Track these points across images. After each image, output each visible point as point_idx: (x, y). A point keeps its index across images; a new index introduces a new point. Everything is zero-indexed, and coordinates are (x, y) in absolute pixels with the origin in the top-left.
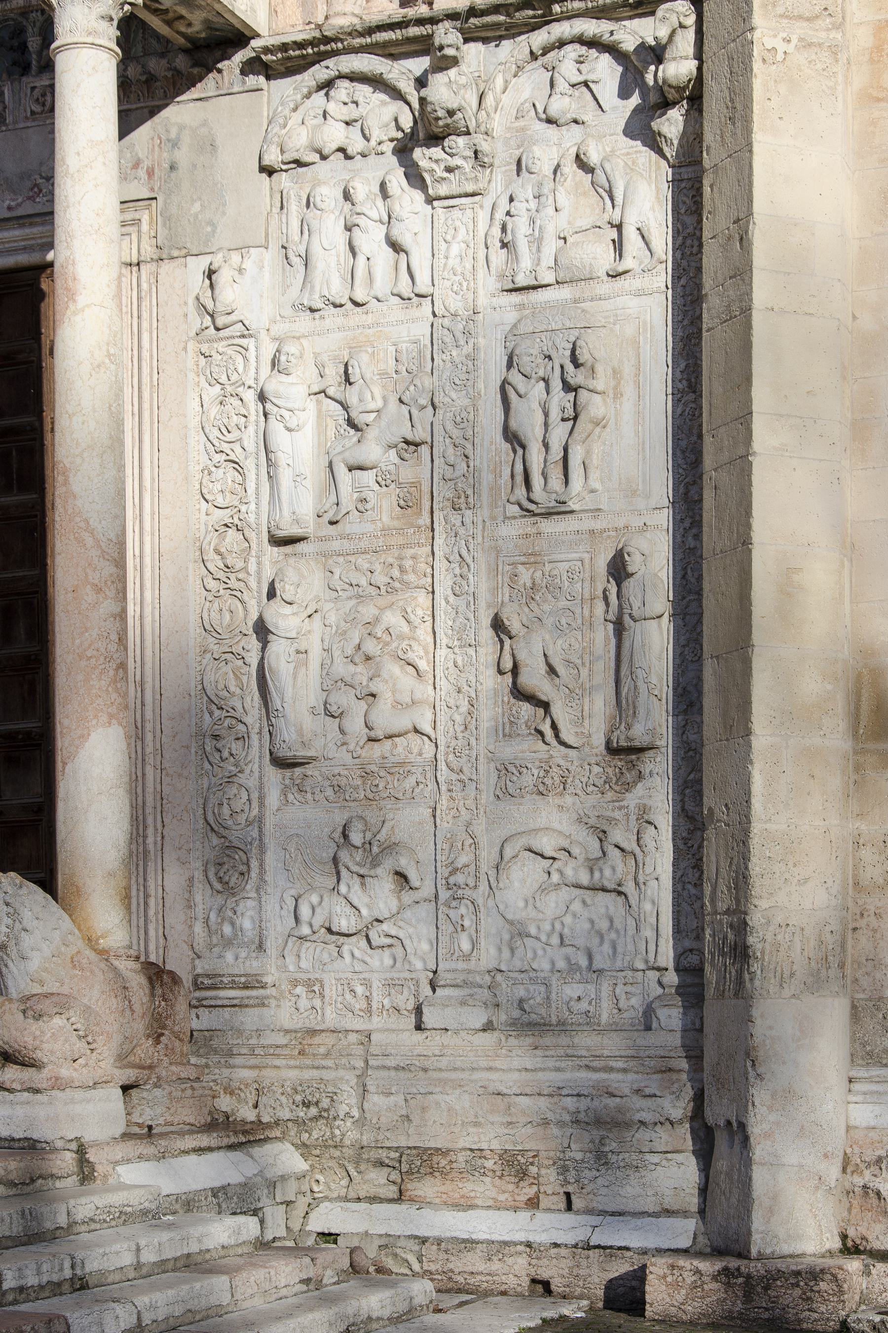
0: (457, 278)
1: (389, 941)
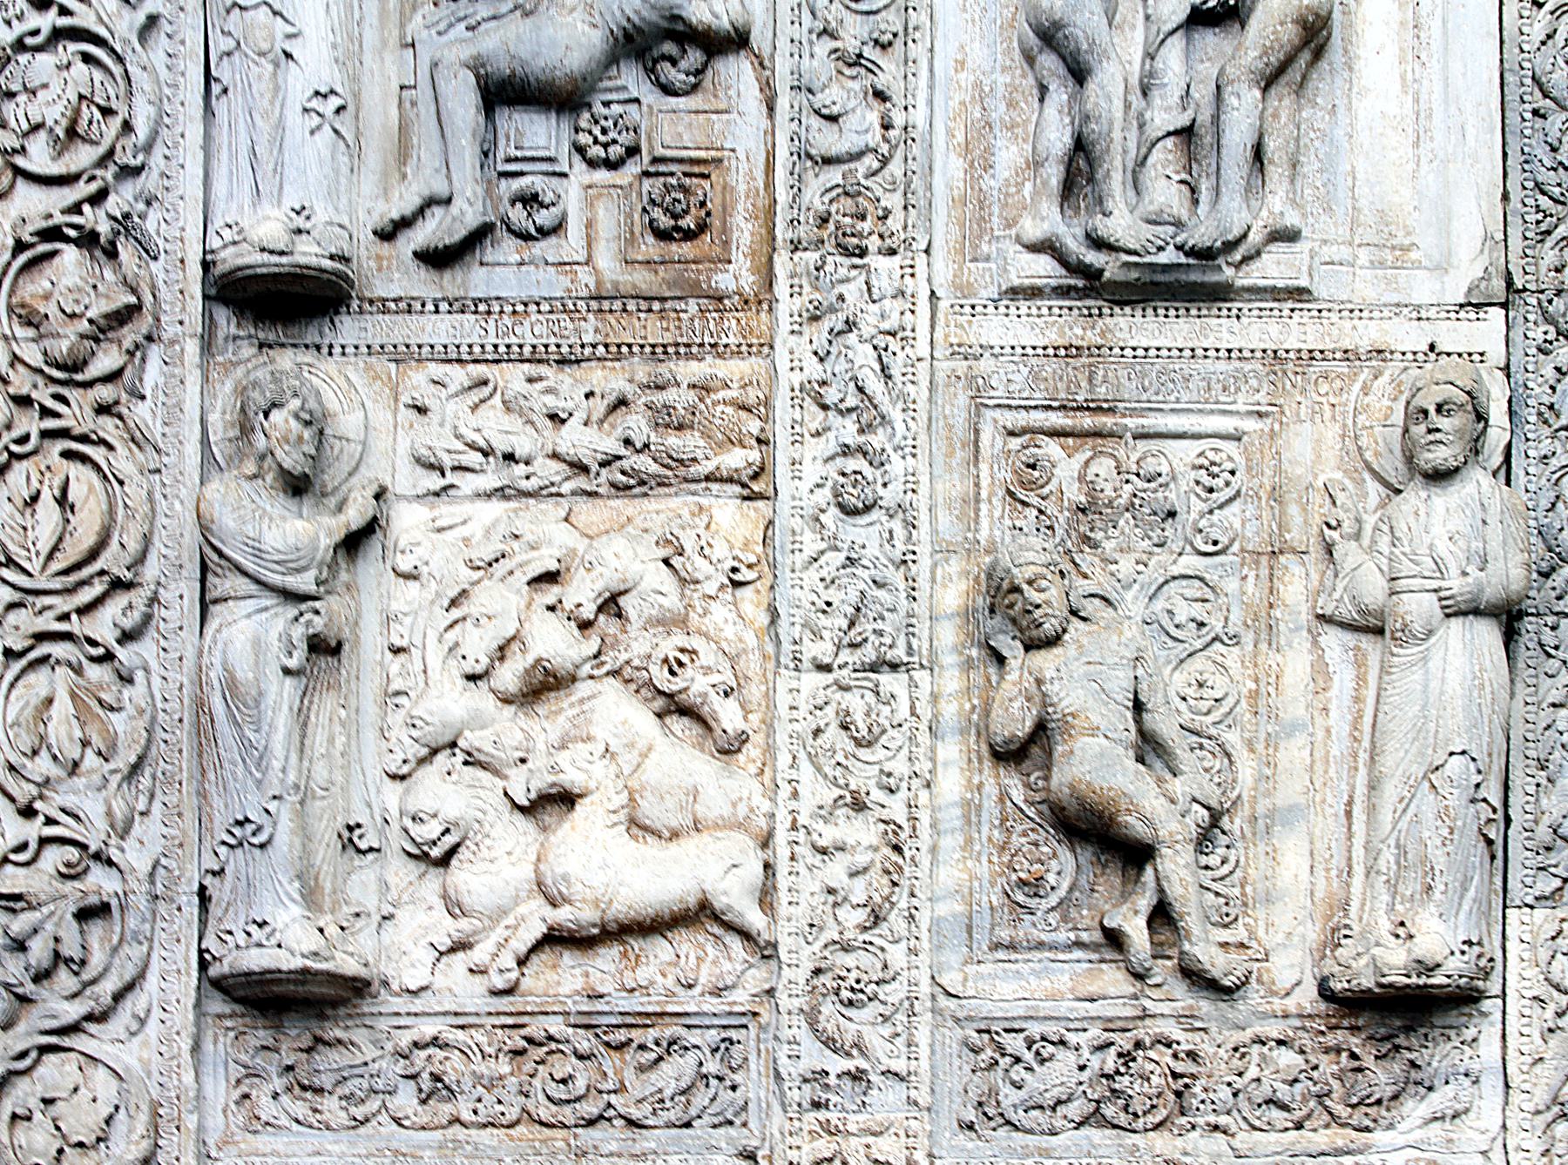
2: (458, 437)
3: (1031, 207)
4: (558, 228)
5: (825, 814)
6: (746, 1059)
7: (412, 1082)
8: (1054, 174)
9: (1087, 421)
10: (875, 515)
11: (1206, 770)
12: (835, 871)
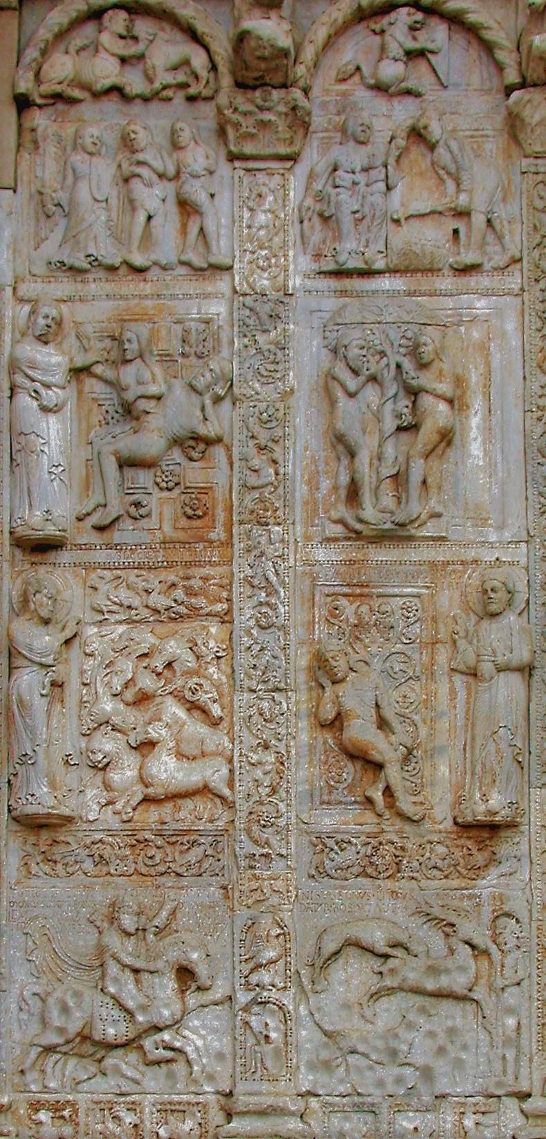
0: (264, 253)
1: (169, 1054)
2: (110, 599)
3: (334, 505)
4: (148, 515)
5: (253, 749)
6: (223, 849)
7: (91, 858)
8: (343, 493)
9: (358, 591)
10: (273, 629)
11: (407, 732)
12: (259, 773)
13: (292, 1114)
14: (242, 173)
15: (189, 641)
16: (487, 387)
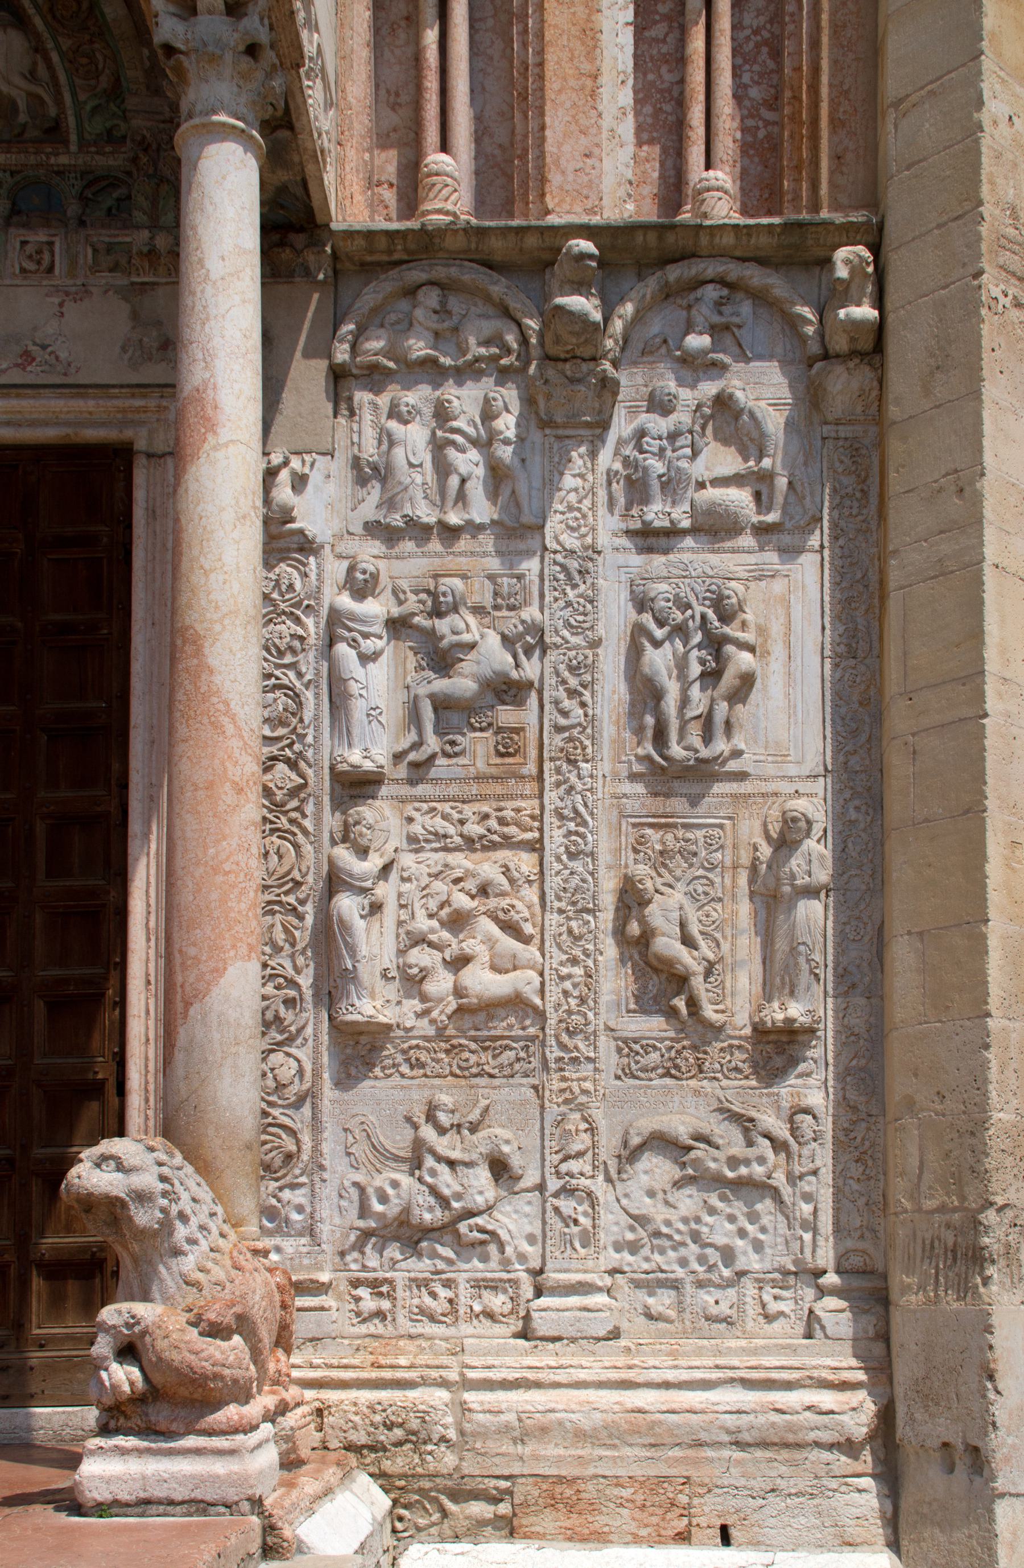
5: (561, 964)
12: (568, 985)
13: (600, 1289)
14: (553, 439)
15: (502, 866)
16: (788, 633)
